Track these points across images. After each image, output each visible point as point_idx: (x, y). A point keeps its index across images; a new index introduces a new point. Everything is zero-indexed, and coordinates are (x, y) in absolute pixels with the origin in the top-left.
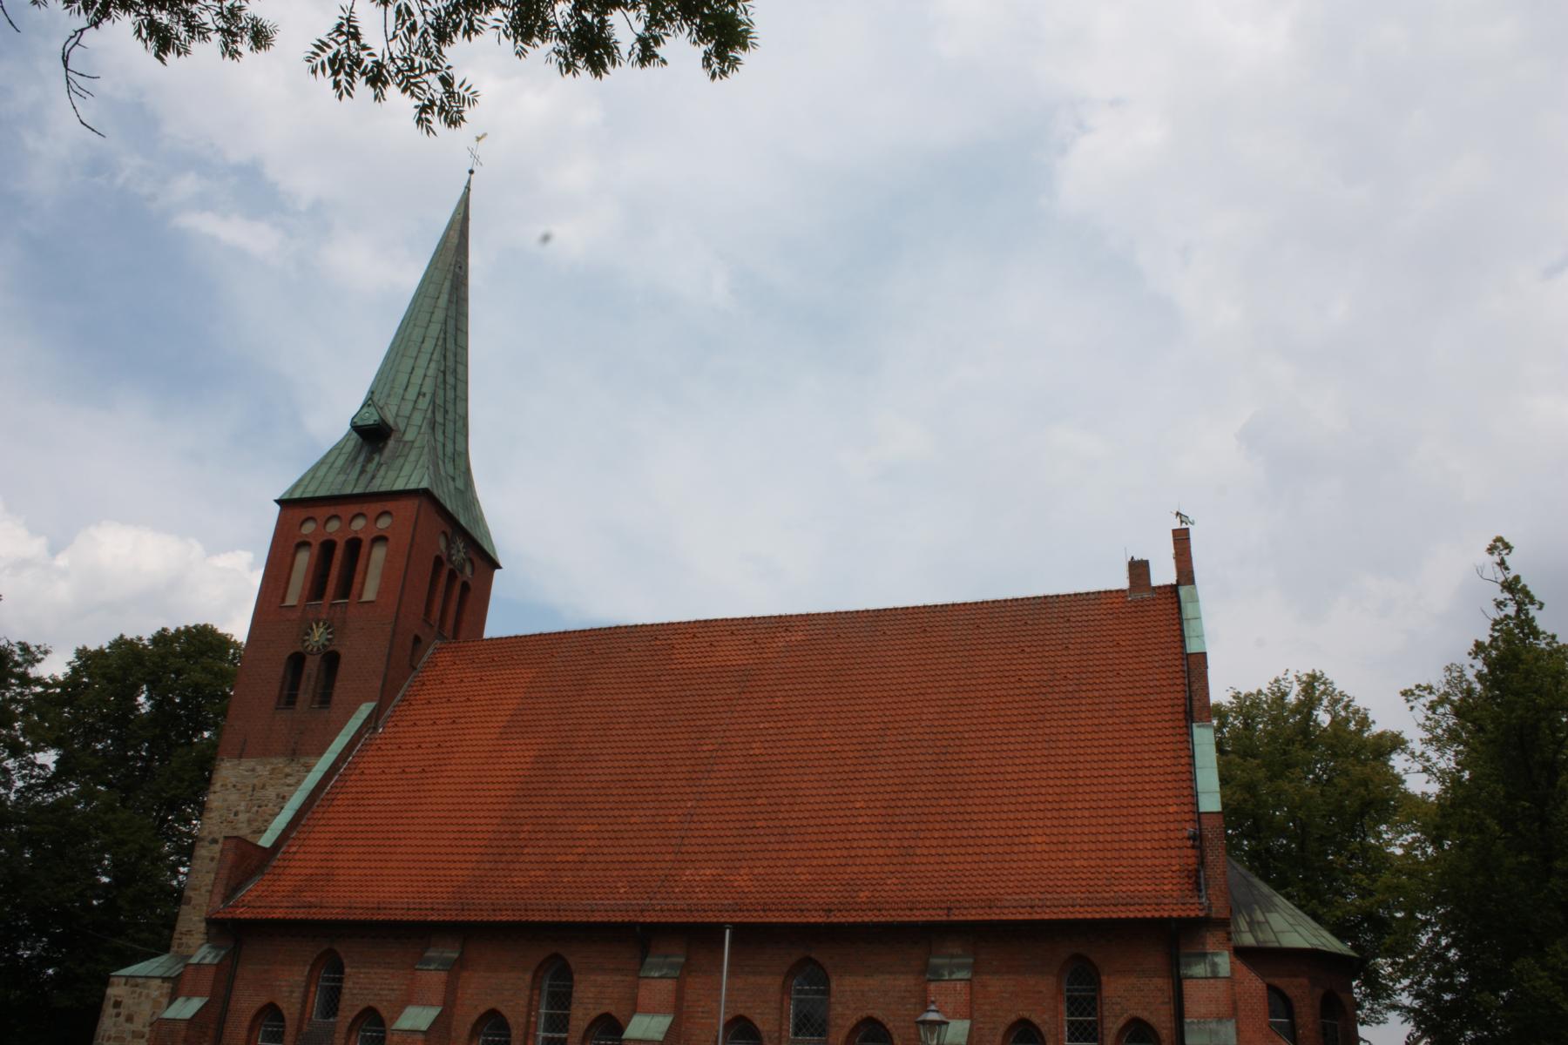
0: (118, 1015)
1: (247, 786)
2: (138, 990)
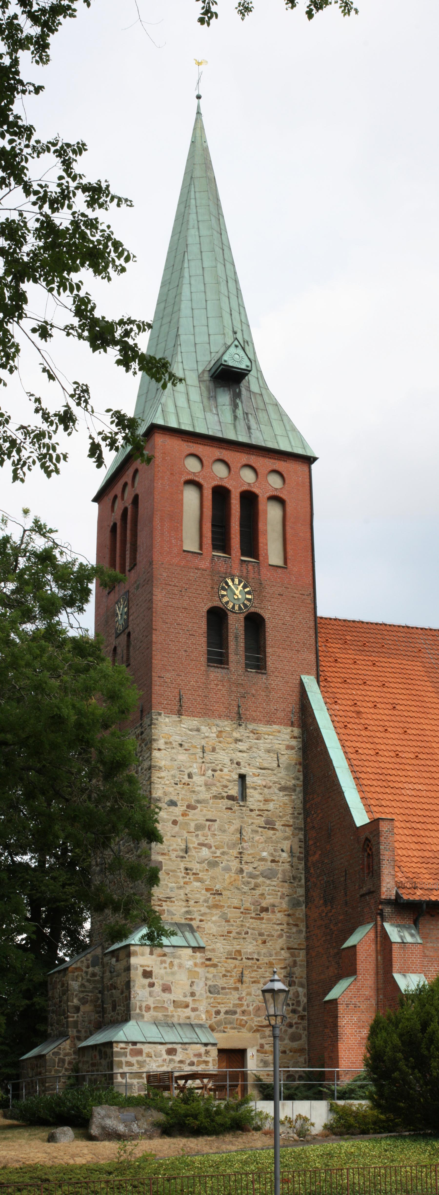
0: (152, 985)
1: (195, 747)
2: (168, 960)
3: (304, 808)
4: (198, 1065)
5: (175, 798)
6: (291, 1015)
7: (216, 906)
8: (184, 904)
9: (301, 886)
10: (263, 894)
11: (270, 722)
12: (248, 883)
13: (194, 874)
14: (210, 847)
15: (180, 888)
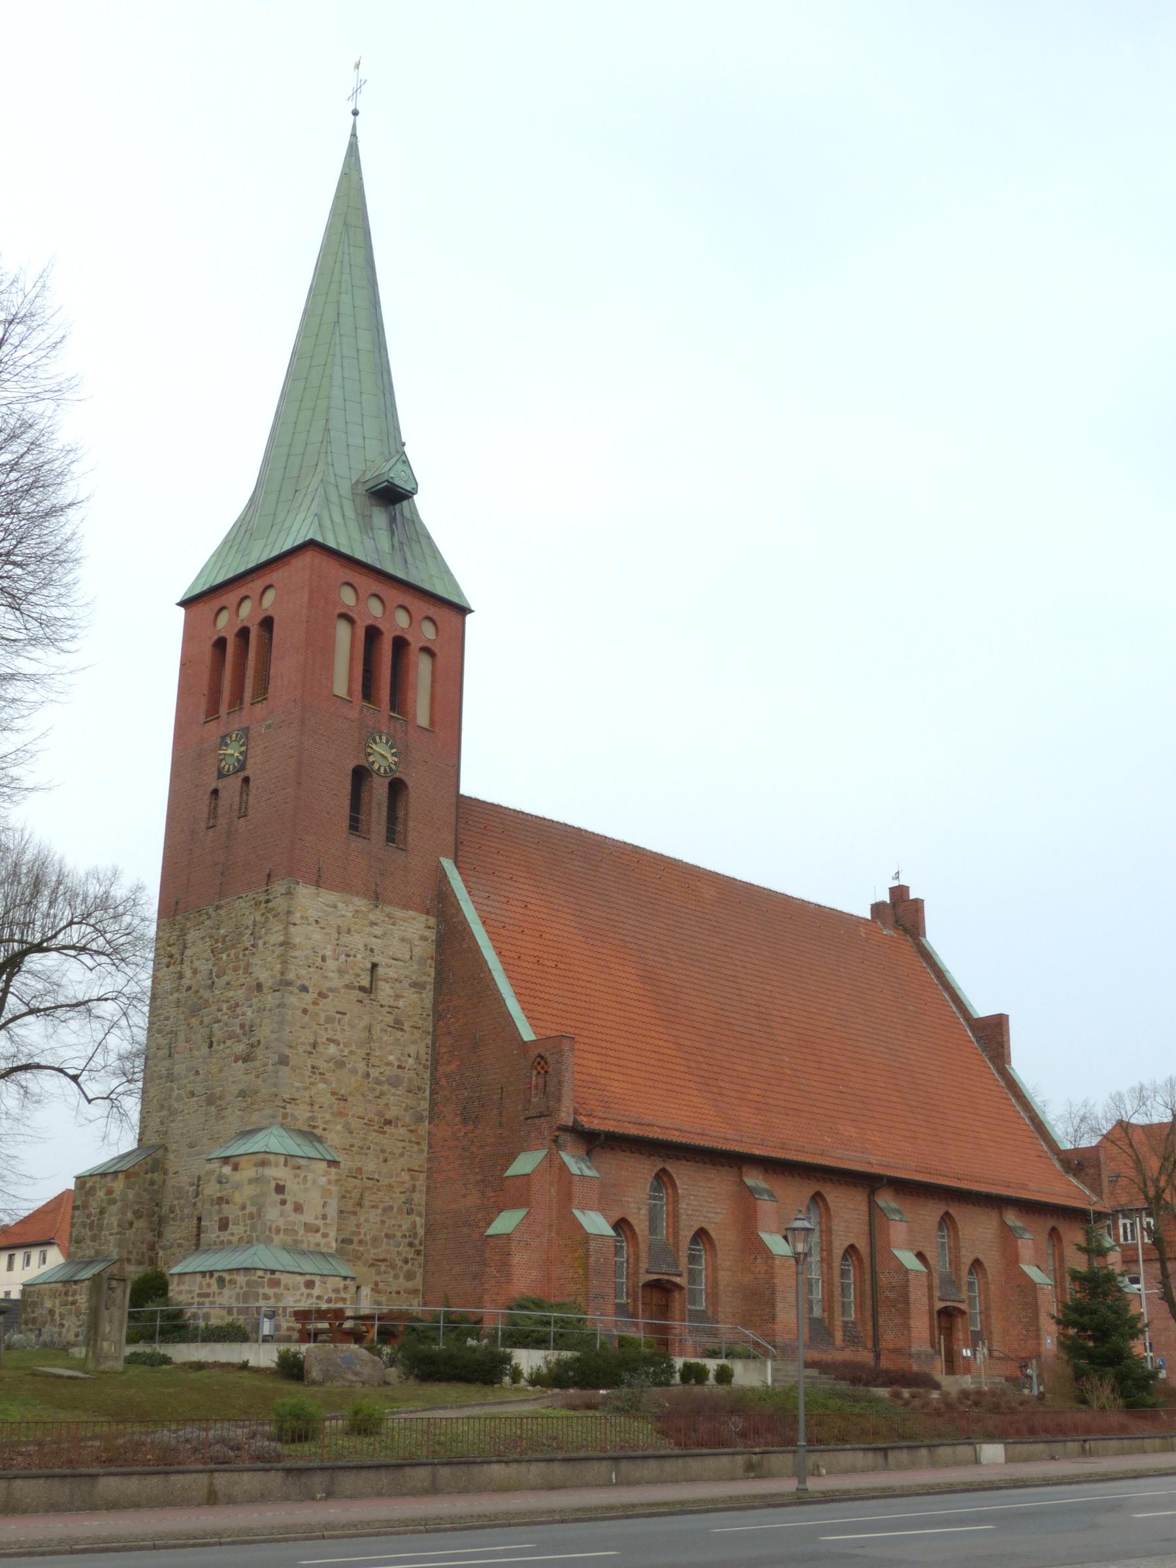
0: (283, 1202)
3: (435, 1010)
4: (335, 1303)
5: (307, 983)
6: (407, 1249)
7: (340, 1114)
8: (308, 1108)
9: (424, 1099)
10: (387, 1105)
11: (406, 907)
12: (374, 1090)
13: (321, 1074)
14: (339, 1044)
15: (306, 1089)
